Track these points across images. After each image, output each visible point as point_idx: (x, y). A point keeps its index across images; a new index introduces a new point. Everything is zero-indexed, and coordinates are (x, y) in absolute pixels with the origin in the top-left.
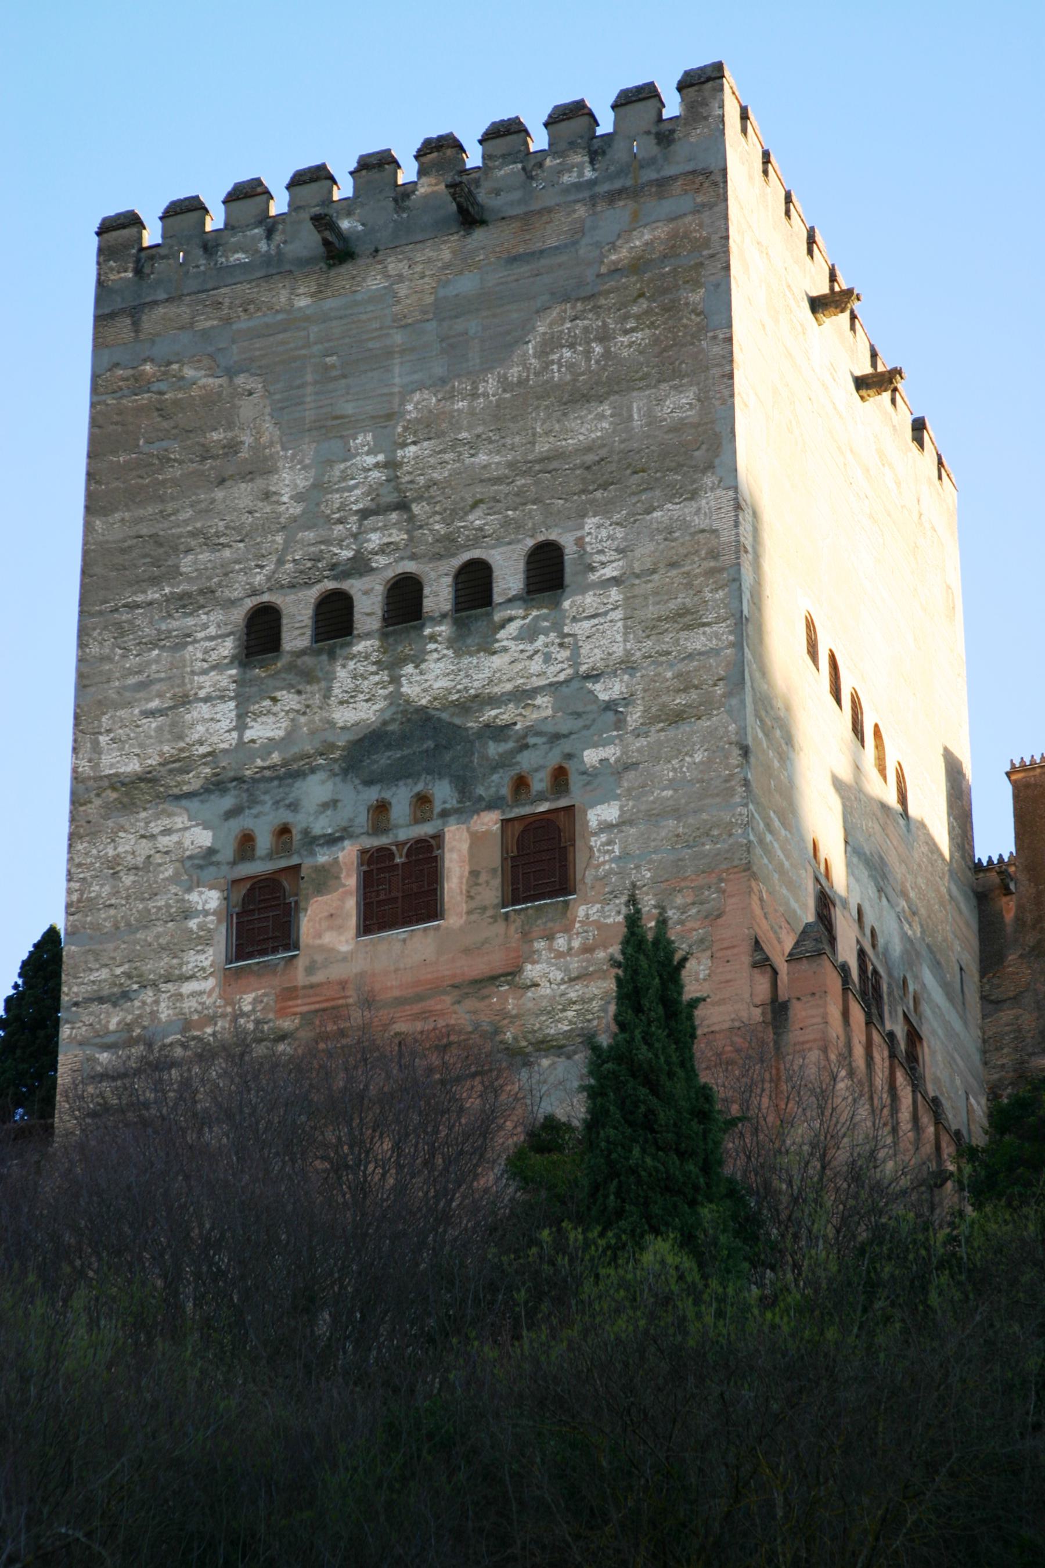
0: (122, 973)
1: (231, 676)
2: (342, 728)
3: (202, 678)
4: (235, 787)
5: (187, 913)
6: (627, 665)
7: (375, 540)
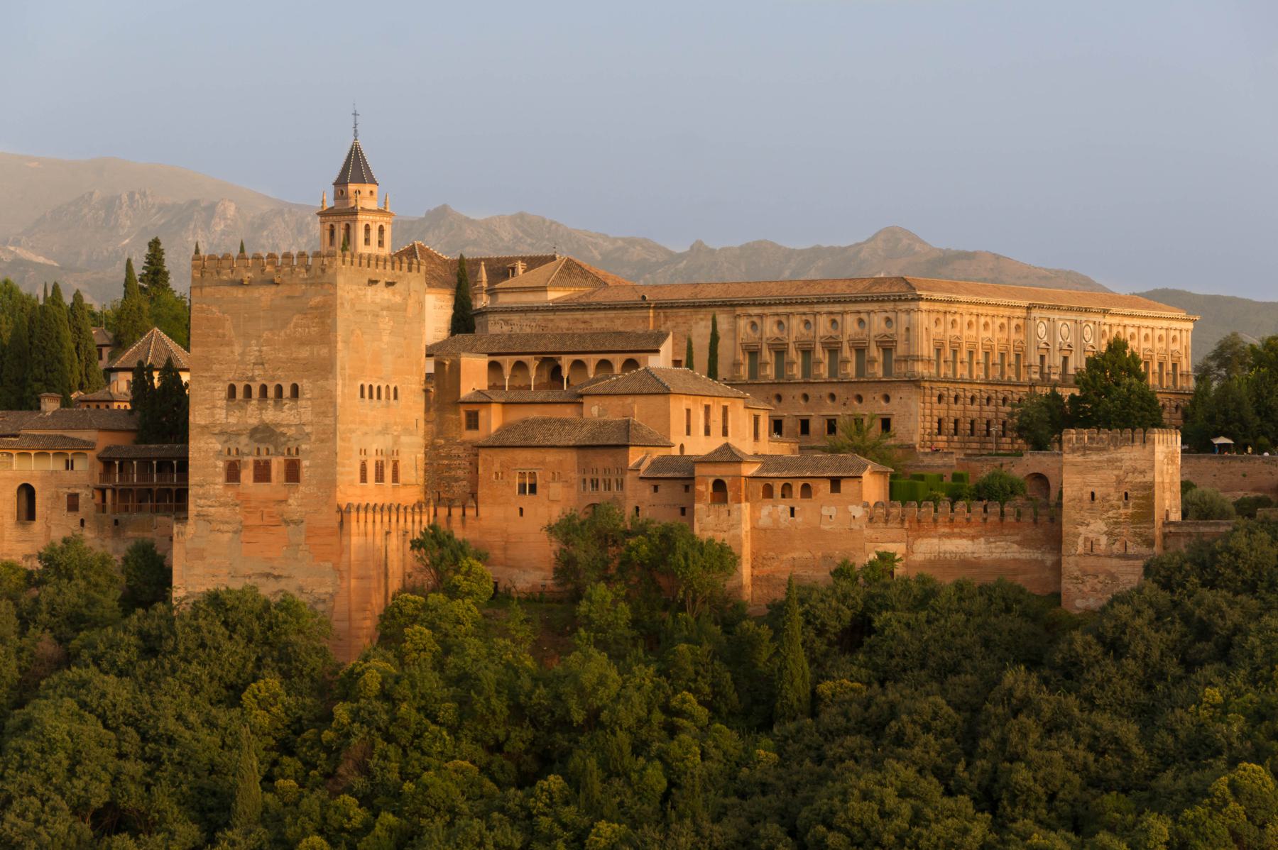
6: (312, 424)
7: (257, 372)
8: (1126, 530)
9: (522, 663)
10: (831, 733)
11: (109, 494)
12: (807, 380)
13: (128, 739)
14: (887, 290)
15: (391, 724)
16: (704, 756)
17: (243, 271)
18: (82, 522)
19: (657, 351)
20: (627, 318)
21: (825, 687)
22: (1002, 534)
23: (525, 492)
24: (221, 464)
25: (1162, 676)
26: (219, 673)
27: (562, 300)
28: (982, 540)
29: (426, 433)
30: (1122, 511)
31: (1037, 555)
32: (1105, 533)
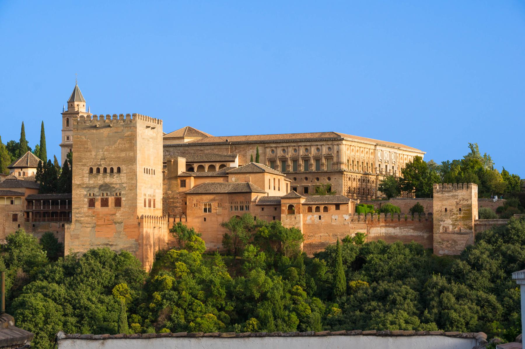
7: (102, 163)
8: (460, 224)
9: (225, 275)
10: (362, 300)
11: (31, 214)
12: (296, 172)
13: (68, 308)
14: (328, 136)
15: (178, 300)
16: (312, 310)
17: (96, 122)
18: (19, 226)
19: (234, 161)
20: (219, 149)
21: (353, 284)
22: (406, 226)
23: (207, 212)
24: (86, 200)
25: (498, 277)
26: (102, 281)
27: (191, 142)
28: (398, 228)
29: (163, 189)
30: (458, 215)
31: (421, 234)
32: (451, 224)
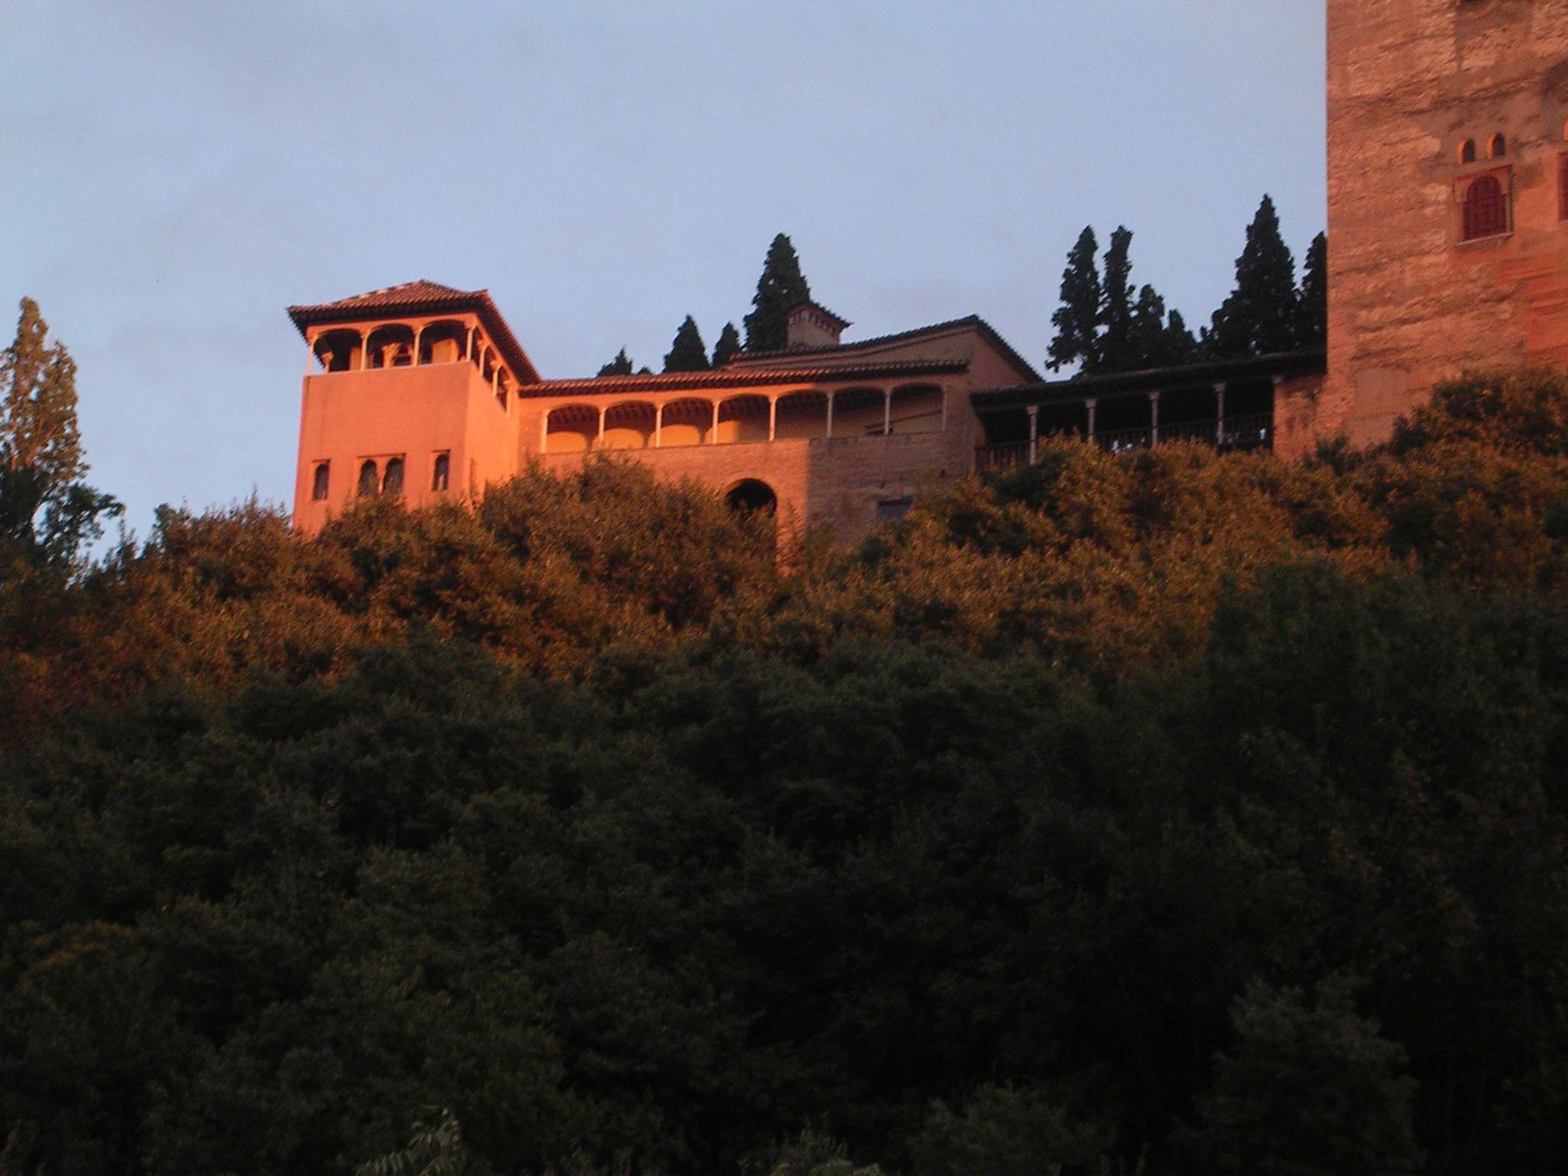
0: (1375, 249)
1: (1449, 18)
2: (1541, 58)
3: (1428, 20)
4: (1456, 106)
5: (1423, 204)
